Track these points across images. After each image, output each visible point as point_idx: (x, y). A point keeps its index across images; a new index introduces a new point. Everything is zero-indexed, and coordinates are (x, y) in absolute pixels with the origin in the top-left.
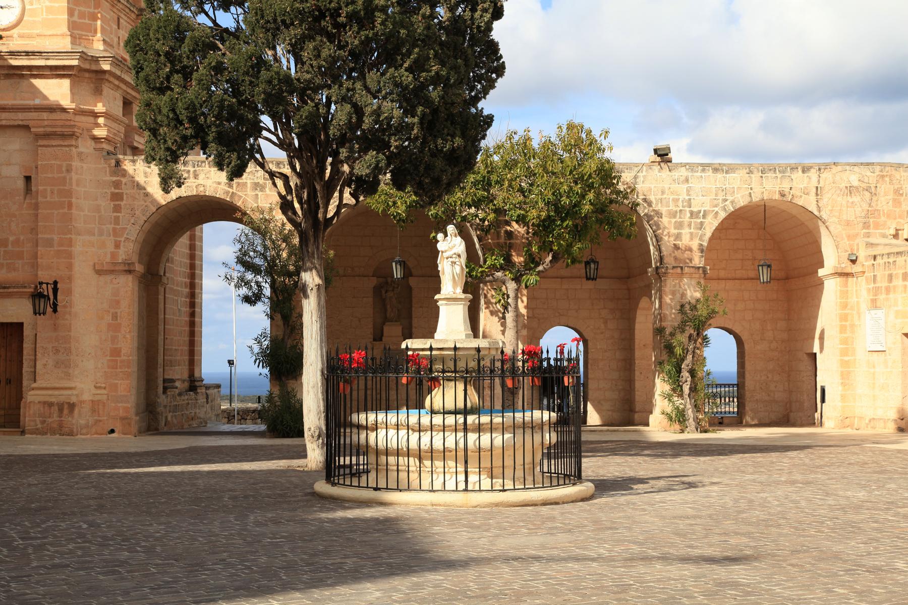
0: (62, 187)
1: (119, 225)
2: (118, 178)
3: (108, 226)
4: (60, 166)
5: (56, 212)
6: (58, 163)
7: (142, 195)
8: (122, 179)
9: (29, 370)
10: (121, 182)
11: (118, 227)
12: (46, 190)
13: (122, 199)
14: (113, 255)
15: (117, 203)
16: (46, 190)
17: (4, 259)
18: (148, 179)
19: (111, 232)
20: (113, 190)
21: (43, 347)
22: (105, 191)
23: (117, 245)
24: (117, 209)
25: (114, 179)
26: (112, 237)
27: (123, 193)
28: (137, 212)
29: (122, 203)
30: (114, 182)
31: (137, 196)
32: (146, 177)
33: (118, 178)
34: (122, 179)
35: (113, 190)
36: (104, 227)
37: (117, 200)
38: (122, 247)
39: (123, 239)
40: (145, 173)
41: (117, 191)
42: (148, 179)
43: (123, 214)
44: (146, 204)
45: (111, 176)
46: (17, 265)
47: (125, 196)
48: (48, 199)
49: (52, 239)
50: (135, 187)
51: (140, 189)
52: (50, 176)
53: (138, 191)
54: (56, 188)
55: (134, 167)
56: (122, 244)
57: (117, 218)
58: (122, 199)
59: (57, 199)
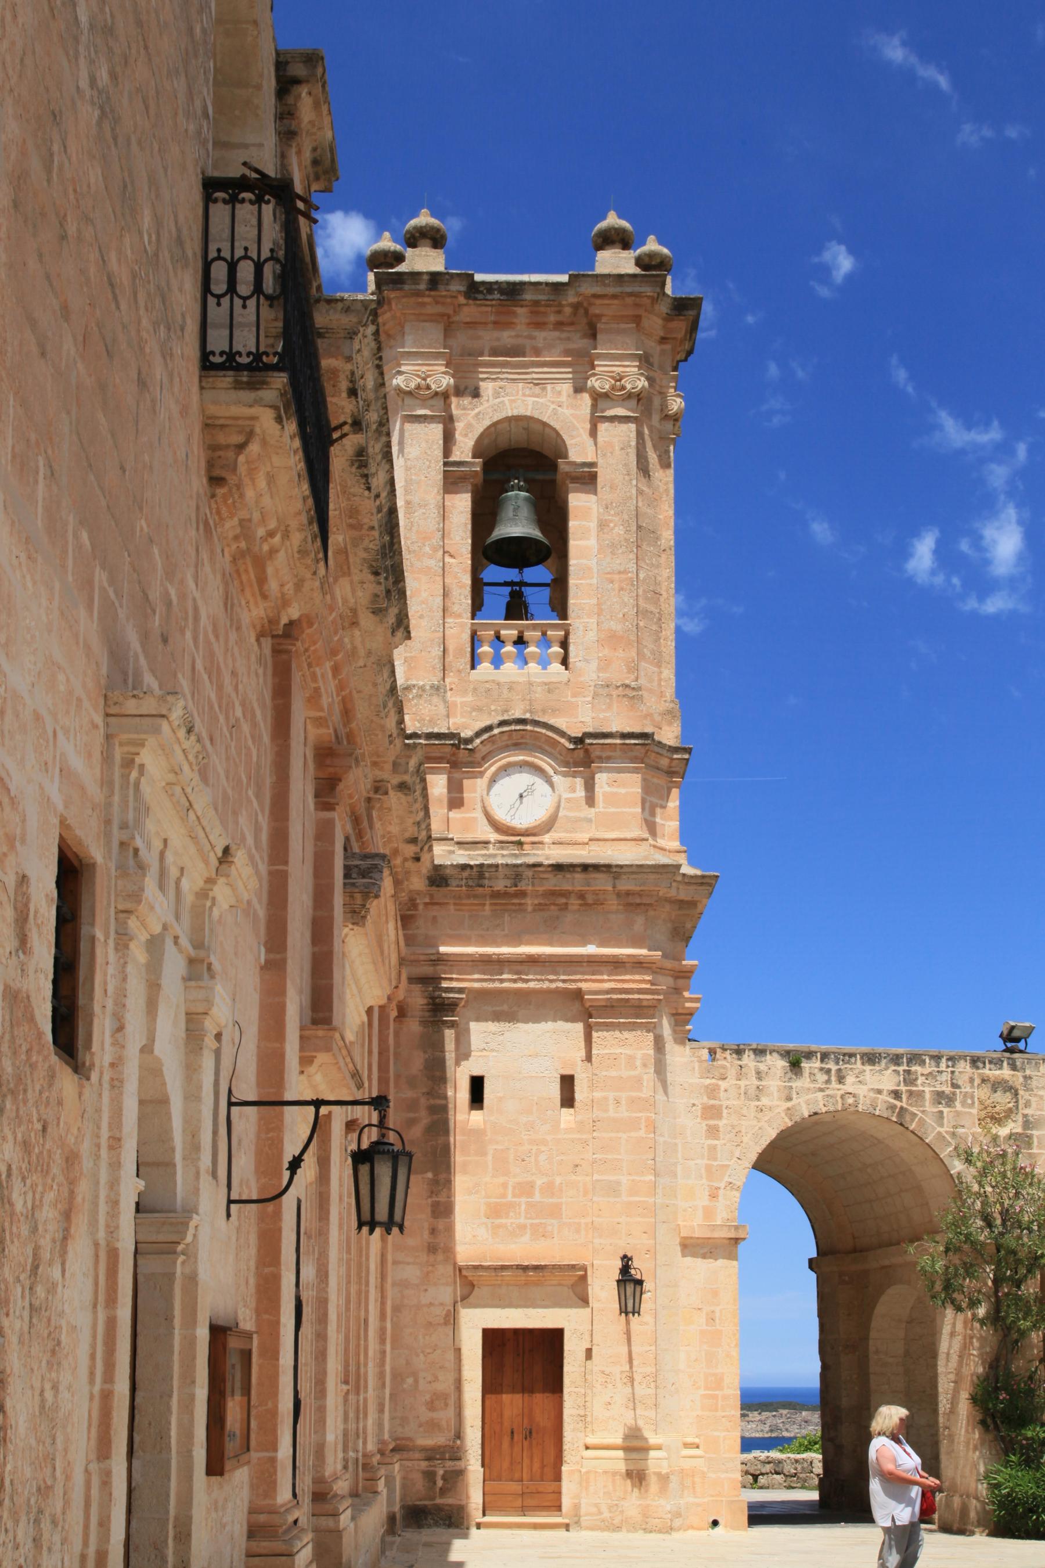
0: (634, 1094)
1: (715, 1159)
3: (698, 1161)
4: (631, 1058)
5: (624, 1136)
6: (628, 1052)
8: (720, 1083)
9: (575, 1412)
11: (715, 1163)
12: (606, 1099)
13: (720, 1116)
14: (708, 1213)
15: (712, 1122)
16: (606, 1099)
17: (526, 1218)
18: (762, 1083)
19: (703, 1171)
21: (603, 1372)
23: (713, 1196)
24: (713, 1132)
25: (708, 1081)
26: (704, 1181)
27: (721, 1106)
28: (745, 1139)
29: (721, 1123)
30: (707, 1087)
31: (745, 1111)
32: (760, 1079)
35: (705, 1099)
36: (691, 1163)
37: (712, 1118)
38: (720, 1198)
39: (722, 1185)
41: (712, 1102)
42: (762, 1083)
43: (723, 1142)
44: (760, 1125)
46: (549, 1228)
47: (725, 1111)
48: (611, 1113)
49: (618, 1183)
52: (614, 1073)
54: (624, 1096)
55: (740, 1063)
56: (721, 1192)
57: (713, 1149)
58: (720, 1116)
59: (626, 1114)
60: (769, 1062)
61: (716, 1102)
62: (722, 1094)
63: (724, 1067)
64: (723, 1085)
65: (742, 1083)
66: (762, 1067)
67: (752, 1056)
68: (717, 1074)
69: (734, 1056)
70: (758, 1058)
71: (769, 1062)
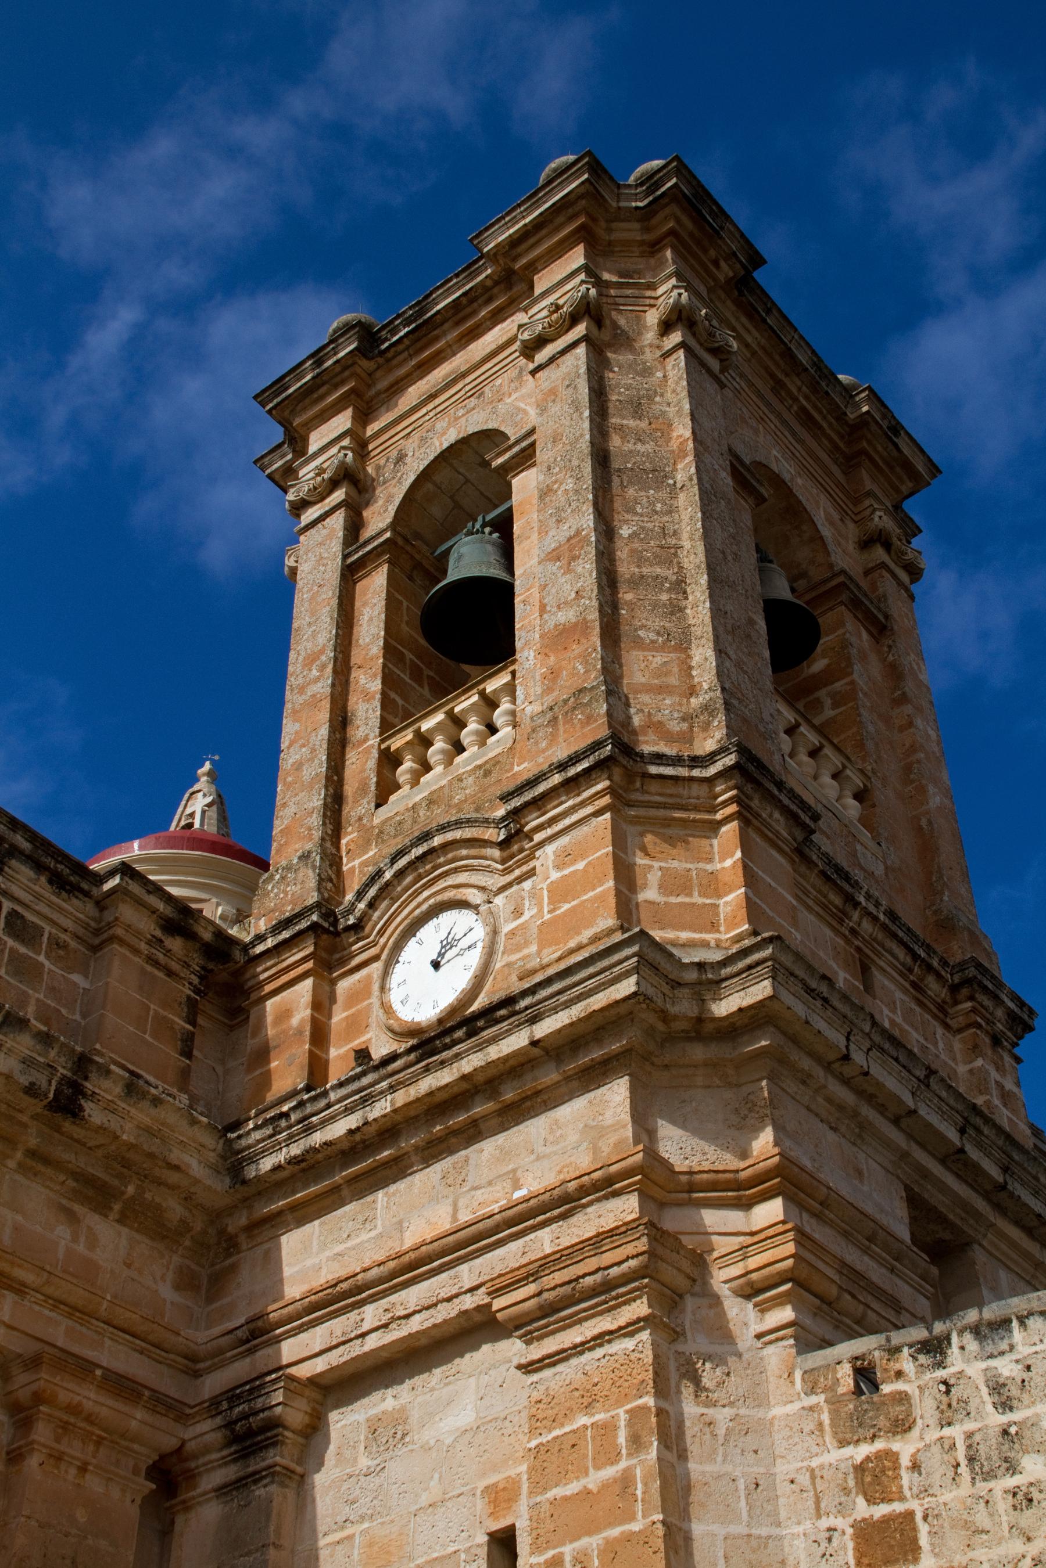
0: (615, 1532)
2: (879, 1445)
6: (600, 1417)
7: (1003, 1505)
8: (896, 1446)
10: (892, 1457)
18: (1016, 1416)
20: (862, 1509)
22: (825, 1523)
25: (862, 1451)
27: (910, 1515)
30: (860, 1469)
31: (982, 1518)
32: (1005, 1405)
33: (879, 1445)
34: (896, 1446)
35: (862, 1509)
40: (997, 1387)
41: (881, 1510)
42: (1016, 1416)
45: (843, 1443)
50: (963, 1469)
51: (989, 1476)
53: (982, 1487)
55: (941, 1374)
60: (1023, 1350)
61: (898, 1507)
62: (906, 1478)
63: (902, 1398)
64: (905, 1448)
65: (956, 1432)
66: (1006, 1368)
67: (972, 1345)
68: (882, 1422)
69: (922, 1359)
70: (990, 1348)
71: (1023, 1350)
